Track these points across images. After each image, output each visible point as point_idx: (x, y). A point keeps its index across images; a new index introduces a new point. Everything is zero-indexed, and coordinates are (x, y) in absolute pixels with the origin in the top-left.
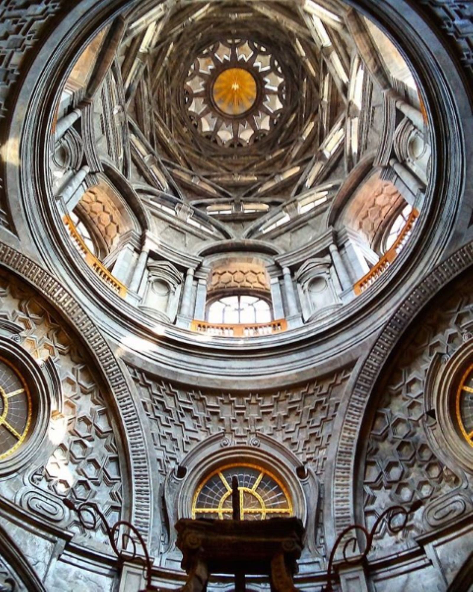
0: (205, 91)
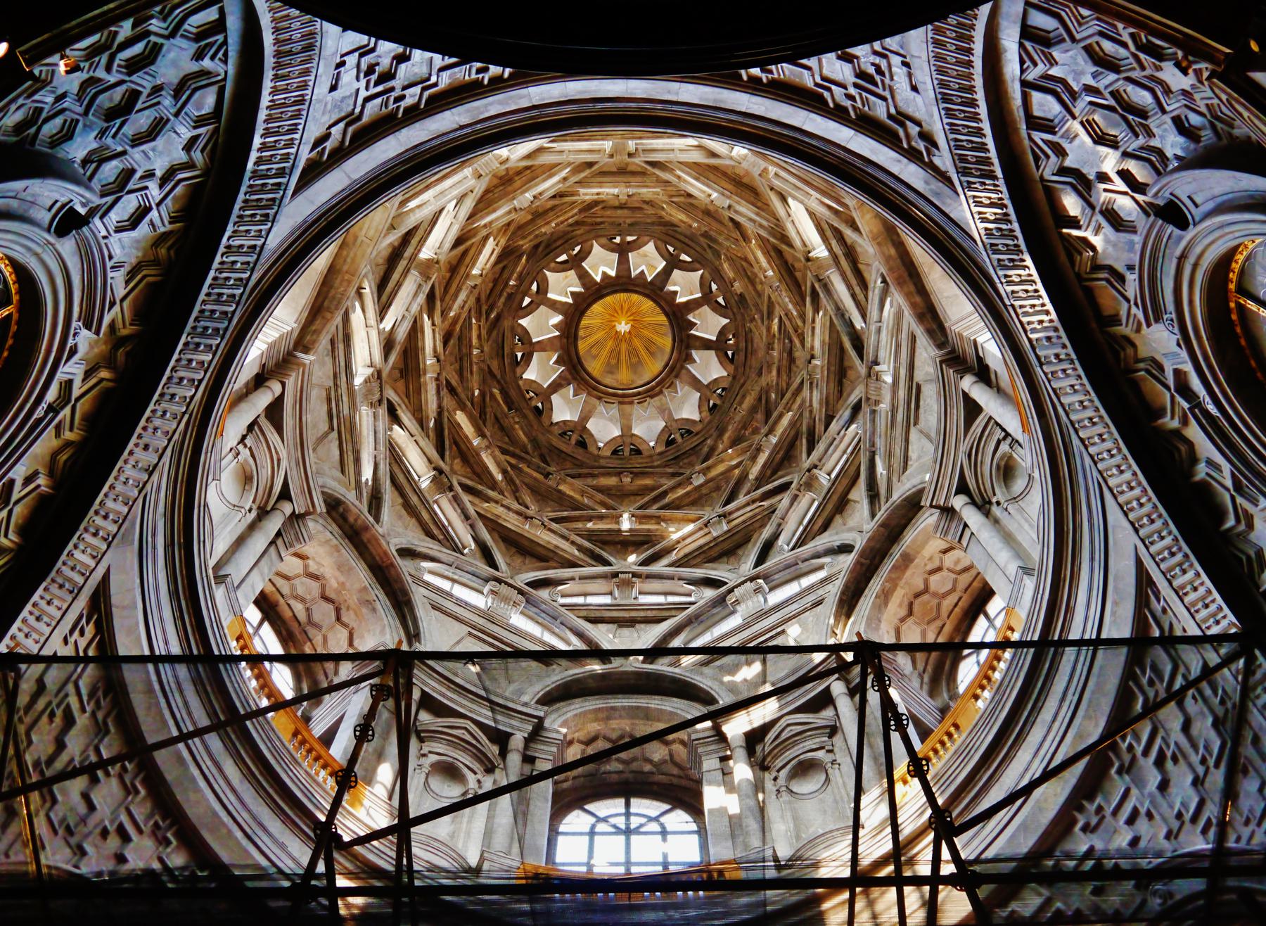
0: (689, 347)
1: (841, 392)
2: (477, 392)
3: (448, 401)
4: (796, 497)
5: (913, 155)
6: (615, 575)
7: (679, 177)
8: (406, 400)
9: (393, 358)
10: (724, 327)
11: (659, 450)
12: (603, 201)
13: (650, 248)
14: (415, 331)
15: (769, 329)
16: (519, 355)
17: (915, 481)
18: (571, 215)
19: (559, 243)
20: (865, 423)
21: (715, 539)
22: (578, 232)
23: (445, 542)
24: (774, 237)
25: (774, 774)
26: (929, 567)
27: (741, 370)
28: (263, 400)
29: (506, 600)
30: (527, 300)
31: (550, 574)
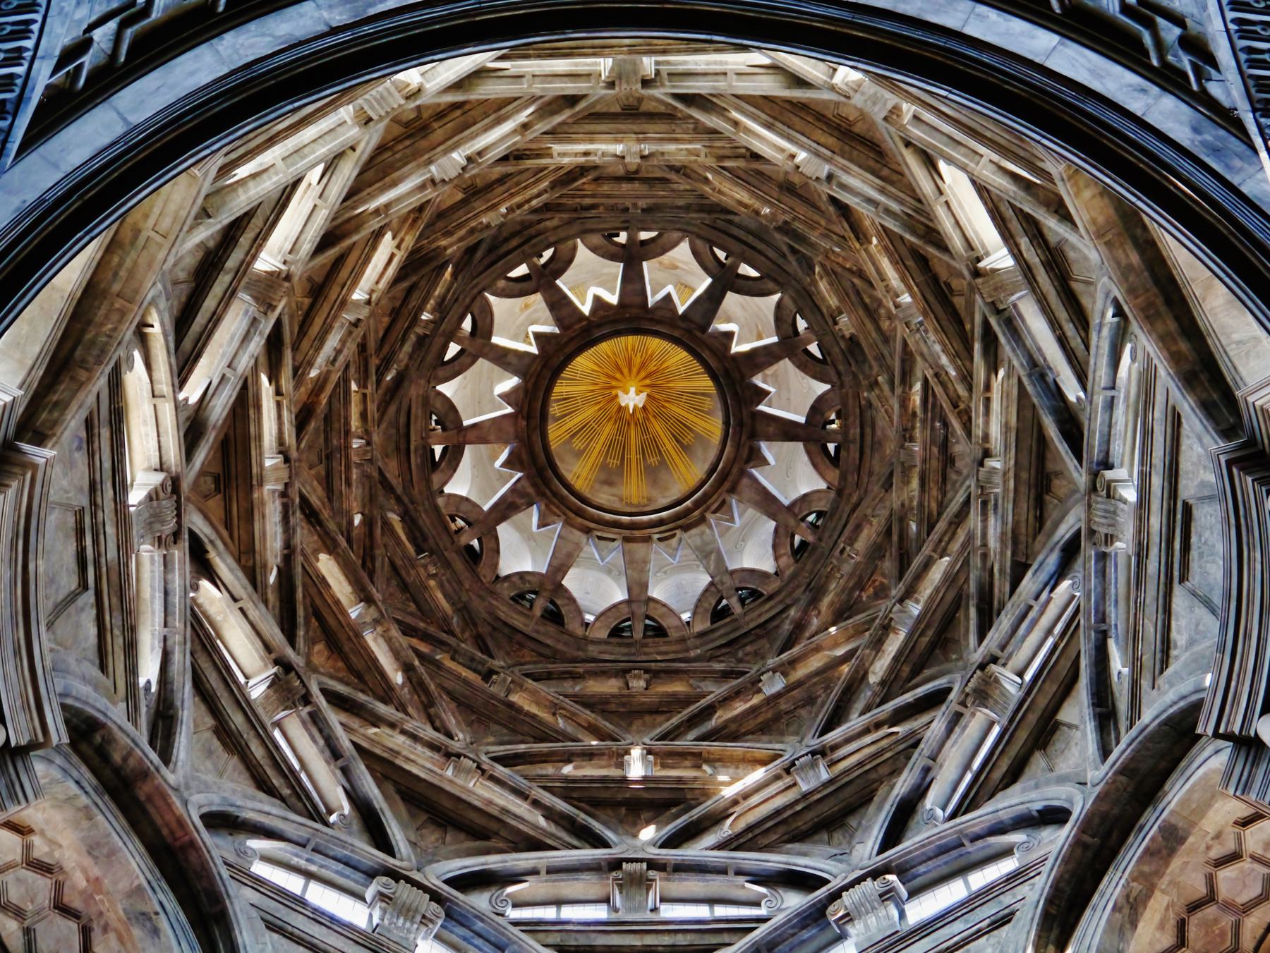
0: (754, 436)
1: (1040, 520)
2: (357, 519)
3: (304, 536)
4: (956, 718)
5: (1169, 80)
6: (616, 864)
7: (736, 124)
8: (225, 533)
9: (201, 456)
10: (821, 399)
11: (699, 627)
12: (596, 167)
13: (682, 252)
14: (245, 403)
15: (904, 401)
16: (438, 449)
17: (1185, 687)
18: (537, 193)
19: (514, 242)
20: (1086, 578)
21: (805, 796)
22: (549, 224)
23: (293, 800)
24: (913, 232)
26: (1216, 852)
27: (852, 479)
29: (407, 911)
30: (453, 349)
31: (493, 862)
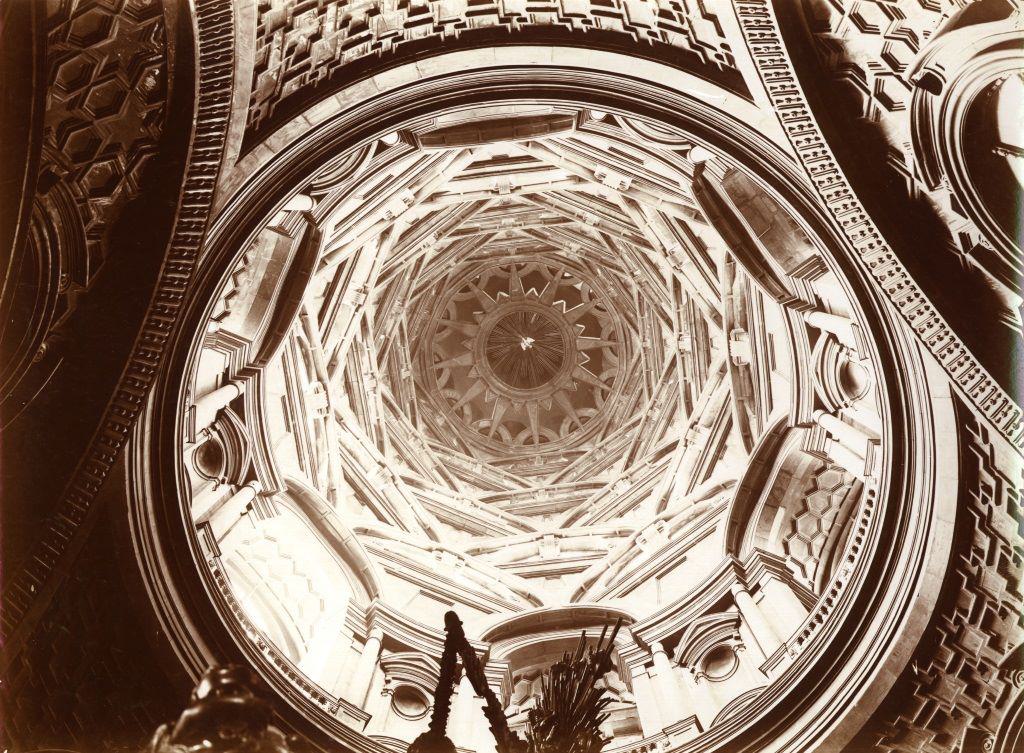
25: (691, 667)
28: (229, 394)
